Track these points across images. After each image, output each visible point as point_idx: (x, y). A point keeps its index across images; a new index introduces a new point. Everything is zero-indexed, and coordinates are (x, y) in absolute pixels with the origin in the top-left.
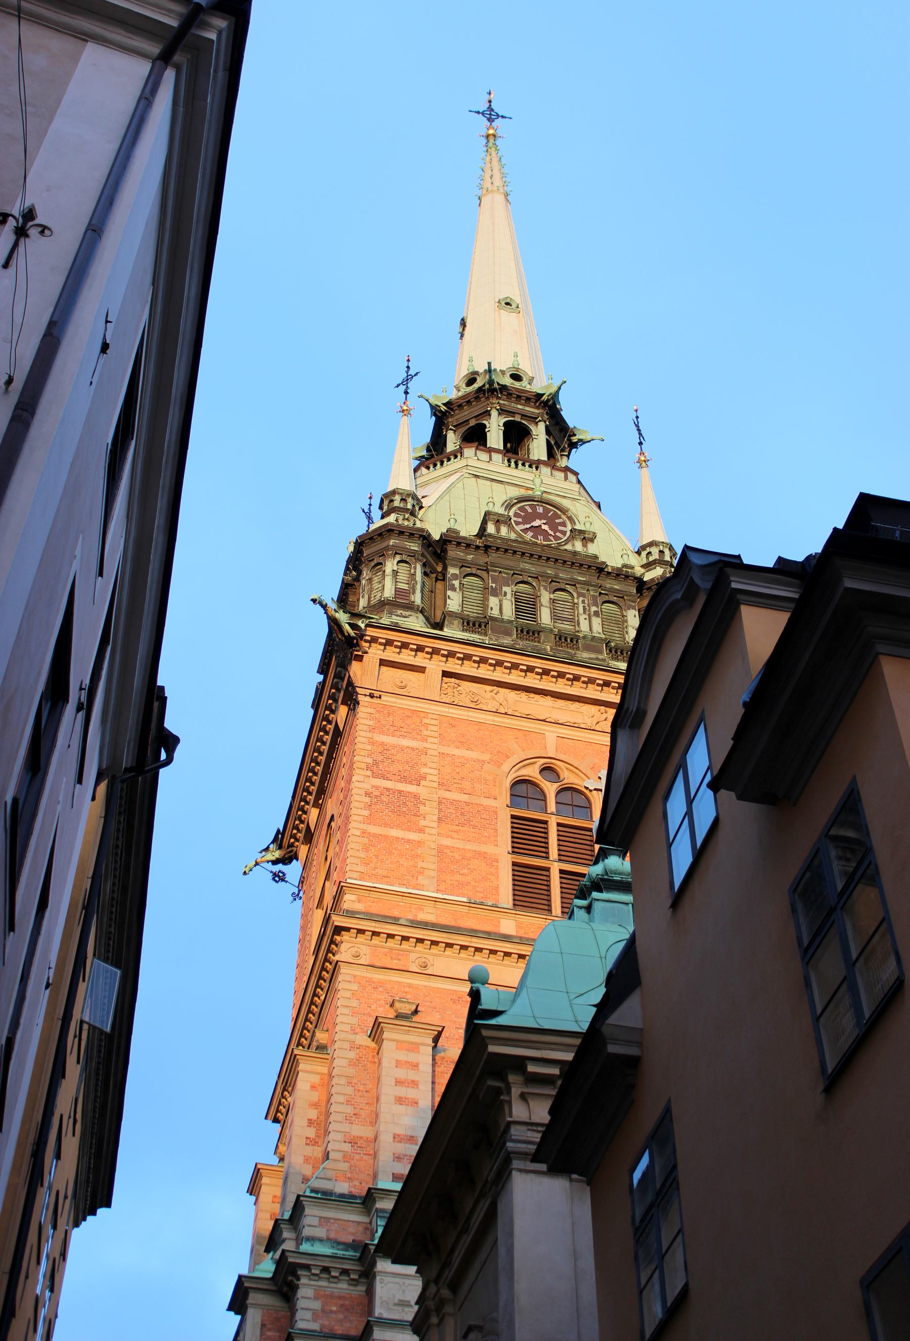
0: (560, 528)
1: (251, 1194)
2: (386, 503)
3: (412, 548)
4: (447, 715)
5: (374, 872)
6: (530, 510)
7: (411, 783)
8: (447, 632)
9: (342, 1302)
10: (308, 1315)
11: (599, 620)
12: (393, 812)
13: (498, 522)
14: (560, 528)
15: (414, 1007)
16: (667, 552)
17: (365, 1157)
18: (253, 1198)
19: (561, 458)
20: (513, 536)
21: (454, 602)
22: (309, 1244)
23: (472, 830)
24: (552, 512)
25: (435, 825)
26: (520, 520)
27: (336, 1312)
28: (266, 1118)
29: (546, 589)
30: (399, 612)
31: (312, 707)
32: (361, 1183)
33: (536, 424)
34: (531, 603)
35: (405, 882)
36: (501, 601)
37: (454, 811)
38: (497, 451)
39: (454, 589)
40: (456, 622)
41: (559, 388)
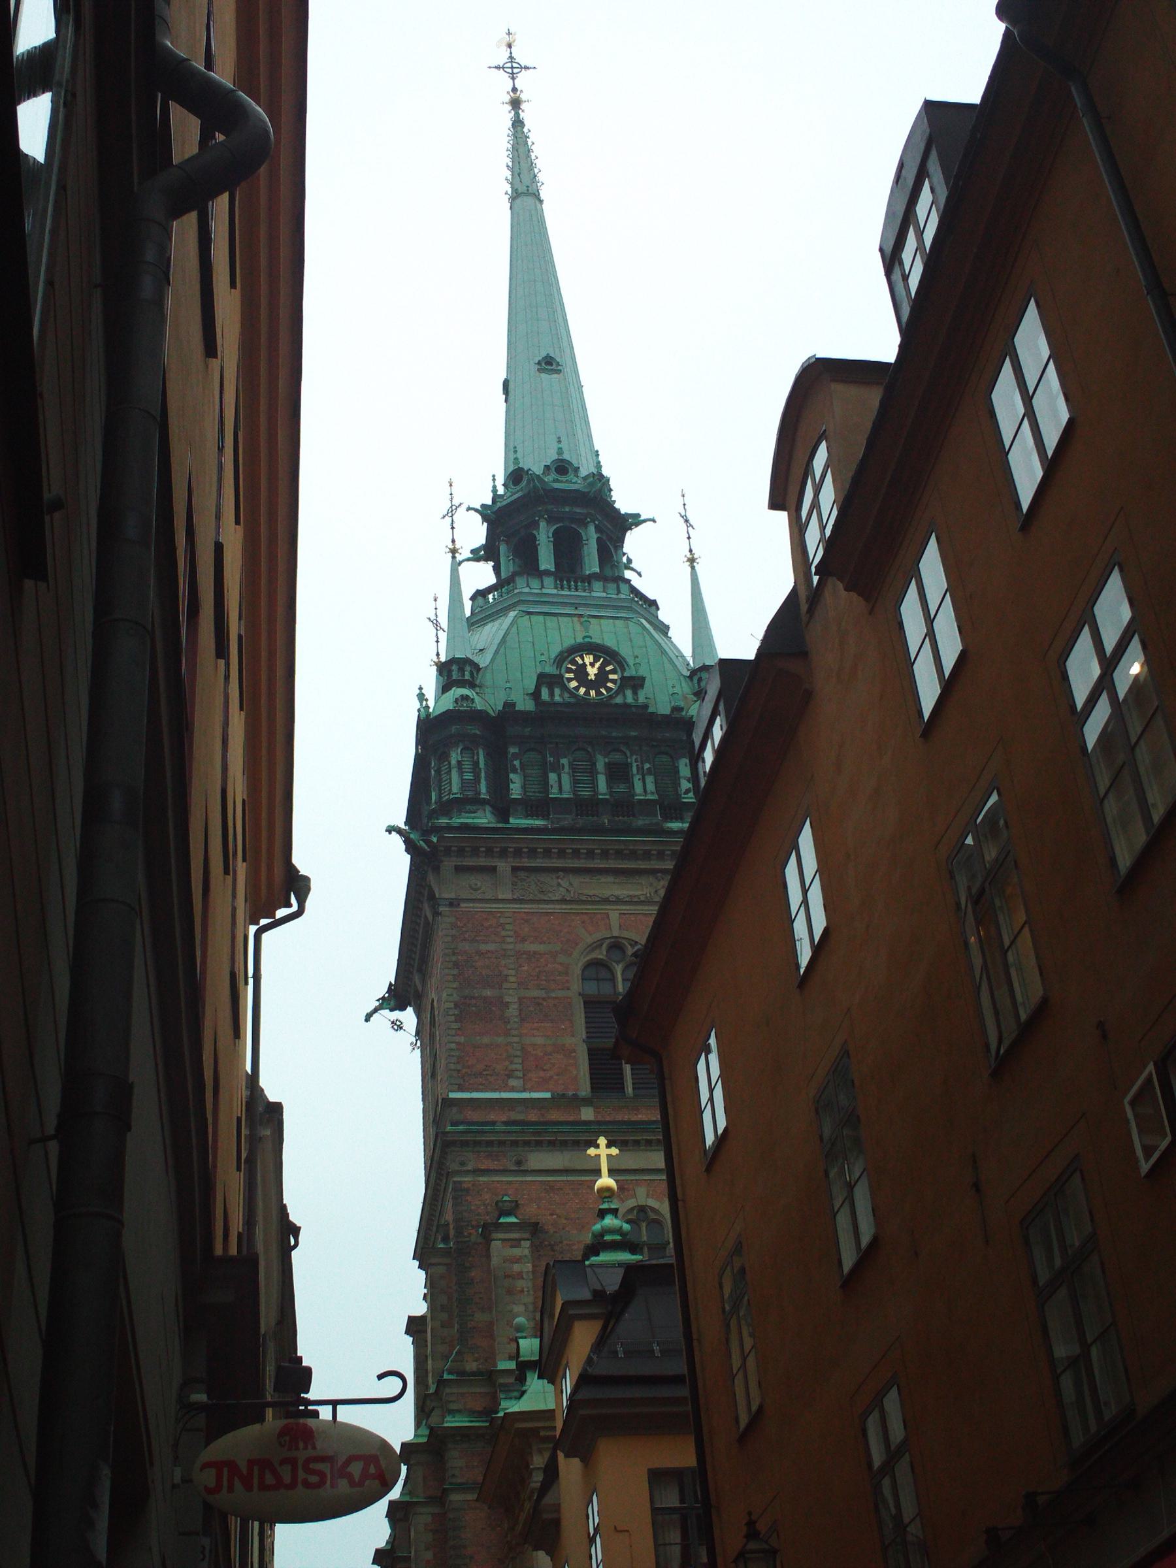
4: (520, 910)
8: (514, 822)
14: (611, 677)
19: (616, 552)
21: (516, 790)
22: (451, 1416)
24: (602, 659)
26: (572, 675)
30: (468, 807)
33: (585, 525)
34: (588, 771)
35: (497, 1087)
38: (547, 573)
39: (515, 771)
40: (519, 808)
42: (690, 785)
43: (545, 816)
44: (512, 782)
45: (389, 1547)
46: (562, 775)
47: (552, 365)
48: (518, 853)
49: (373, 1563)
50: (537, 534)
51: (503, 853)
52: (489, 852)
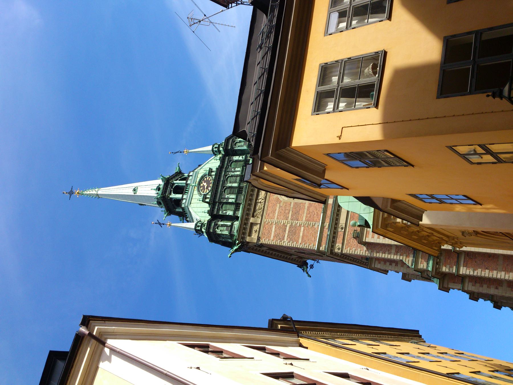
0: (208, 179)
1: (411, 281)
2: (199, 232)
3: (213, 225)
5: (313, 241)
6: (202, 188)
7: (286, 229)
9: (447, 259)
10: (451, 269)
11: (236, 169)
12: (295, 234)
13: (206, 198)
14: (208, 179)
15: (355, 231)
16: (215, 146)
17: (402, 249)
18: (412, 280)
19: (185, 176)
20: (210, 194)
21: (230, 213)
22: (429, 268)
23: (301, 211)
25: (299, 222)
27: (450, 261)
28: (387, 274)
29: (227, 185)
30: (233, 230)
32: (410, 251)
33: (174, 184)
35: (316, 232)
36: (230, 198)
37: (295, 216)
38: (183, 196)
40: (236, 212)
42: (241, 156)
43: (240, 204)
44: (229, 214)
45: (493, 303)
46: (230, 197)
47: (135, 190)
48: (248, 215)
49: (500, 310)
50: (174, 199)
51: (247, 219)
52: (246, 224)
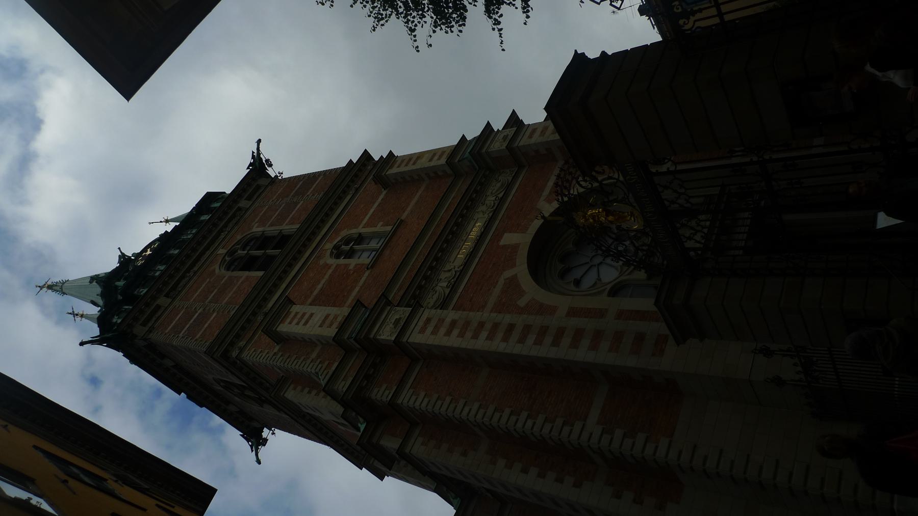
31: (201, 407)
41: (121, 252)
